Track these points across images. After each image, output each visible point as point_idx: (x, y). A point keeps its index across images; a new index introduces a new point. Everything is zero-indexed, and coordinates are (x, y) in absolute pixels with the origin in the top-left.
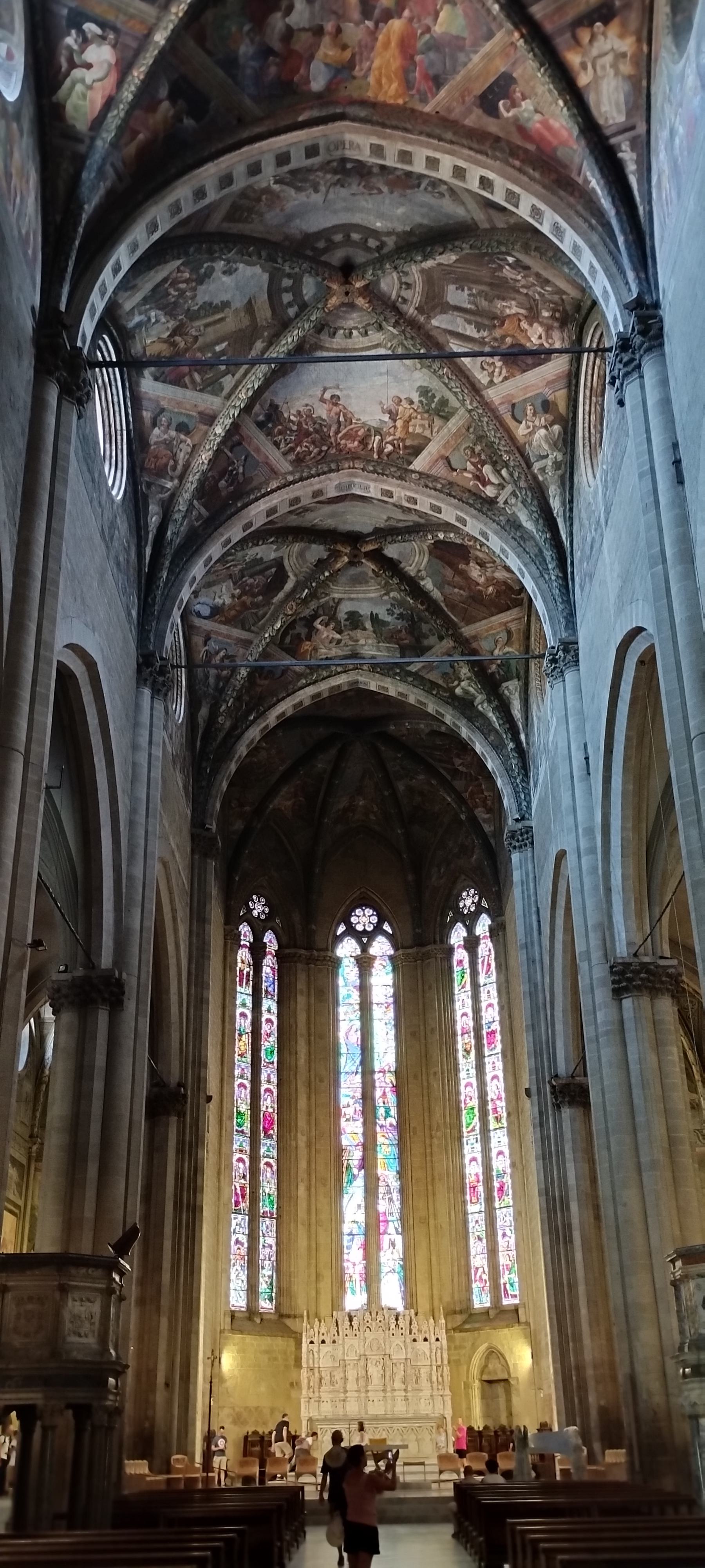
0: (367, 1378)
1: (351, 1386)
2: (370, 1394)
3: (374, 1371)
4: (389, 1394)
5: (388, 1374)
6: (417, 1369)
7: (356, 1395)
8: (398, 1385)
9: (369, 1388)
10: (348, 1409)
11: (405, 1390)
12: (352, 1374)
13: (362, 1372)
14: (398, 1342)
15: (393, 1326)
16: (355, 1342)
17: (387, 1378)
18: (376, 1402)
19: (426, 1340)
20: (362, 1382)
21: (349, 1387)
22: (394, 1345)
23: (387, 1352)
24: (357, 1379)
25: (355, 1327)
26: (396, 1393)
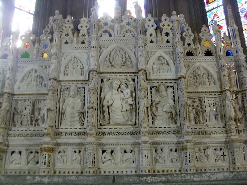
0: (103, 111)
1: (70, 124)
2: (105, 140)
3: (118, 101)
4: (144, 138)
5: (143, 103)
6: (198, 98)
7: (76, 140)
8: (162, 123)
9: (106, 129)
10: (59, 165)
11: (177, 132)
12: (72, 104)
13: (92, 99)
14: (160, 53)
15: (151, 30)
16: (81, 54)
17: (142, 109)
18: (118, 155)
19: (208, 53)
20: (92, 118)
21: (65, 127)
22: (153, 59)
23: (142, 66)
24: (82, 114)
25: (83, 31)
26: (160, 138)
